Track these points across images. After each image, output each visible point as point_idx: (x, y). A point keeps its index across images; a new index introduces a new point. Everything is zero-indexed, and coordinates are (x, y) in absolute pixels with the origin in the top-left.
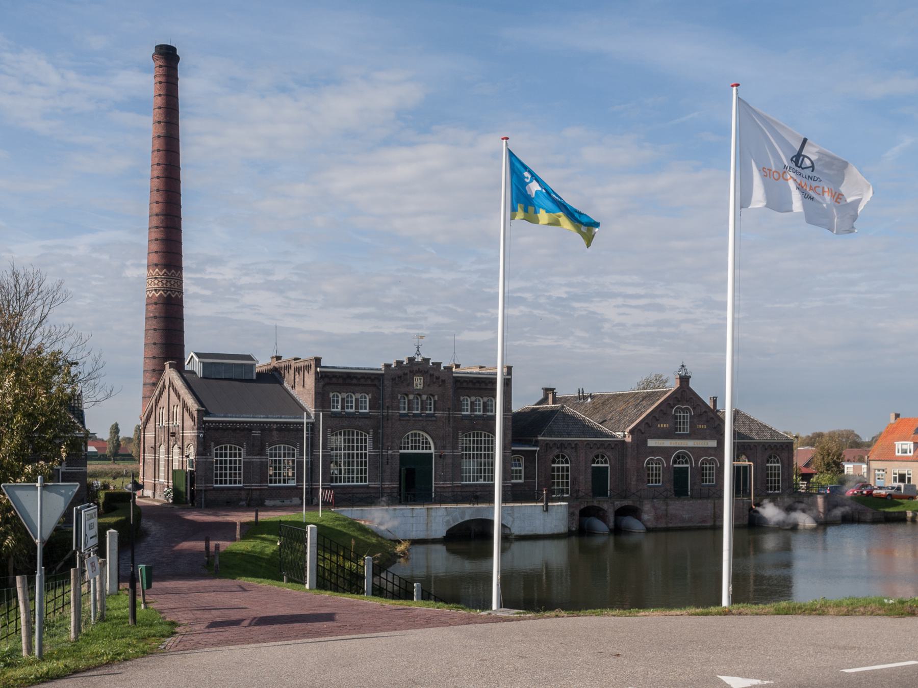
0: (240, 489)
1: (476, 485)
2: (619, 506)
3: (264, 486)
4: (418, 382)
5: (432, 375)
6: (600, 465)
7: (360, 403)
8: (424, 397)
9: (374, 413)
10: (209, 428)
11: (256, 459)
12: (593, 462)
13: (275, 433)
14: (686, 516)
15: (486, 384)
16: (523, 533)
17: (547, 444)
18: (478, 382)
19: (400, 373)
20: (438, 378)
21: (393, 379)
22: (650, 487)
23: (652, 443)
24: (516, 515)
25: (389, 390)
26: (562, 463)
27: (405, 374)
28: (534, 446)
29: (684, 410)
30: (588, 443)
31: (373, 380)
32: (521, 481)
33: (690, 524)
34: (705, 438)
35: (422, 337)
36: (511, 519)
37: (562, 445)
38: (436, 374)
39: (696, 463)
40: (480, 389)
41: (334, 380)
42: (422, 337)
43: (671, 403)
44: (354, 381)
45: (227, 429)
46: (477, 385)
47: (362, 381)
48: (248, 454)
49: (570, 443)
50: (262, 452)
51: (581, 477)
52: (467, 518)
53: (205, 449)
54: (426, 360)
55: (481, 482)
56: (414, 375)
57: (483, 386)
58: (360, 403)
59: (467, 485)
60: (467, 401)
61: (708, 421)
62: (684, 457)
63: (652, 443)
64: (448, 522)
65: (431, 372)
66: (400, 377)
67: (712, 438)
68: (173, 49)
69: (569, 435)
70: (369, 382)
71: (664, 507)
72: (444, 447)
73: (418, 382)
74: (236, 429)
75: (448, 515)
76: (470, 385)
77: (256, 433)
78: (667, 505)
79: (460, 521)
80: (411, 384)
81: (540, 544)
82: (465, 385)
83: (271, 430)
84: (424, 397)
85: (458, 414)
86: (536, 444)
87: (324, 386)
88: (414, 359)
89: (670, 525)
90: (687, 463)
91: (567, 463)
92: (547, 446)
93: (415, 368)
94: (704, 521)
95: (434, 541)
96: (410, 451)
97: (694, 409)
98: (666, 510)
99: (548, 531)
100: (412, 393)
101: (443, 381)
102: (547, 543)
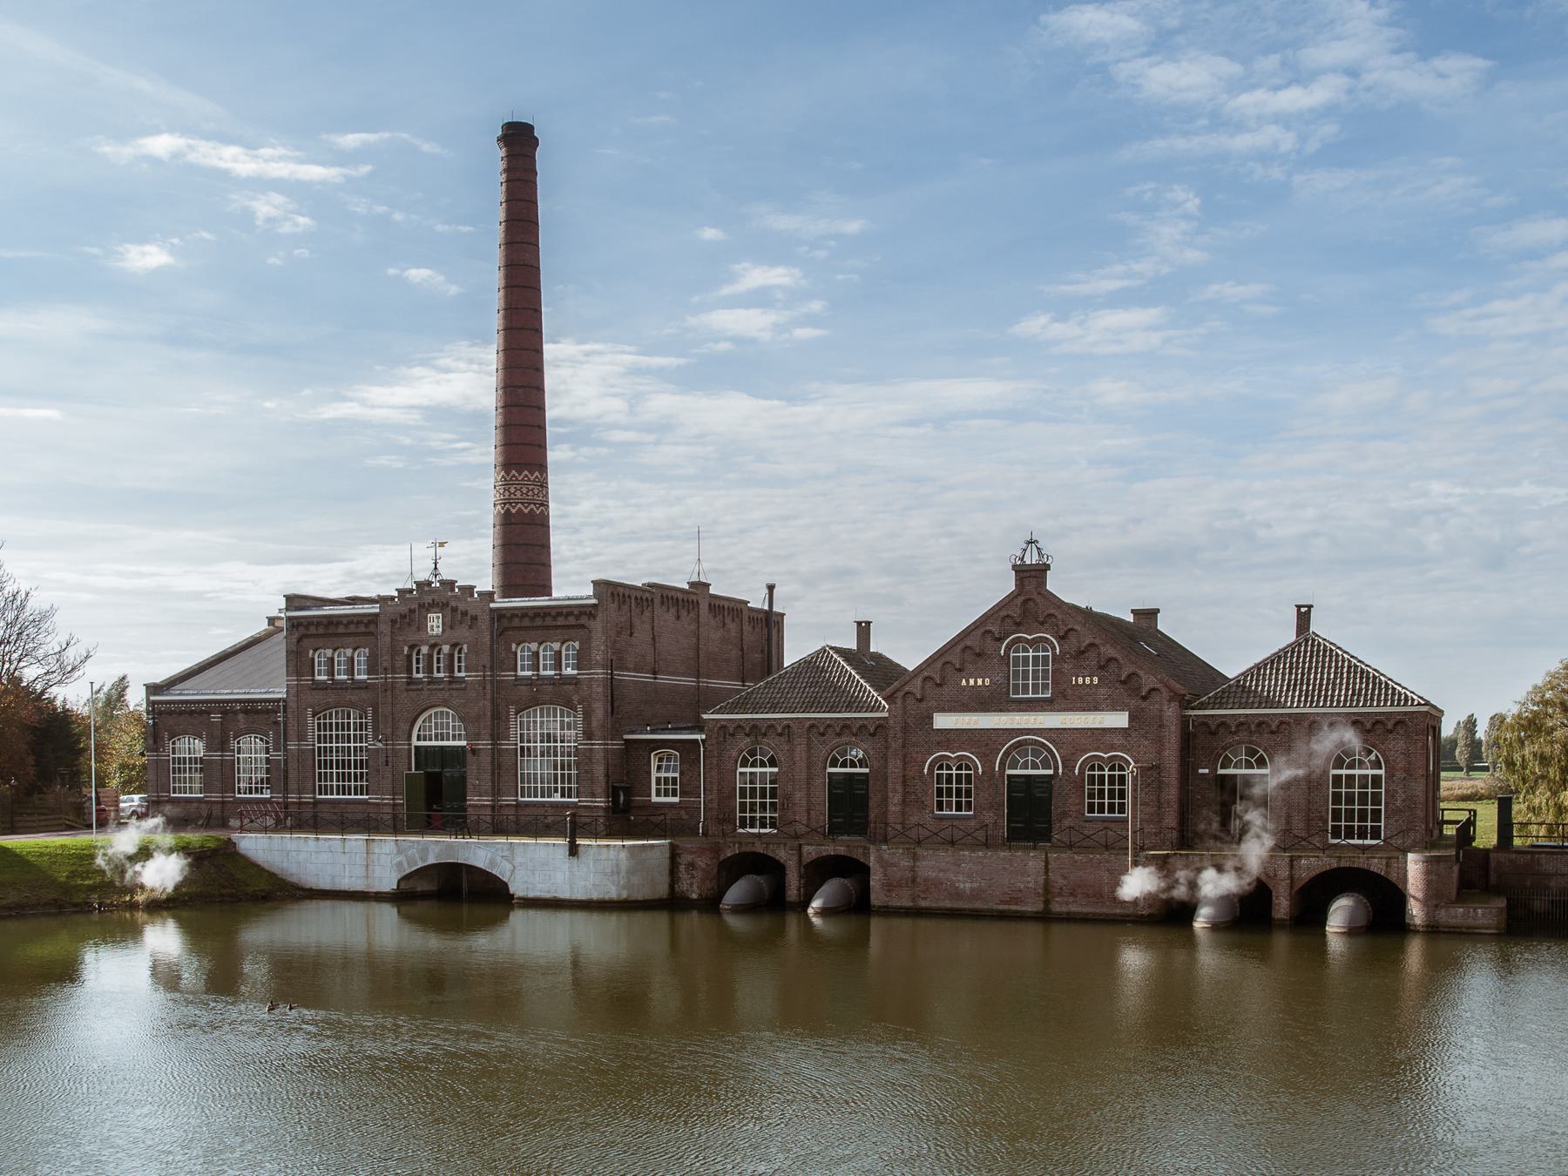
0: (198, 800)
1: (543, 804)
2: (814, 856)
3: (229, 797)
4: (435, 623)
5: (455, 610)
6: (848, 770)
7: (349, 664)
8: (446, 649)
9: (378, 679)
10: (161, 713)
11: (216, 756)
12: (834, 765)
13: (241, 716)
14: (966, 886)
15: (555, 618)
16: (531, 895)
17: (723, 727)
18: (537, 615)
19: (404, 609)
20: (465, 614)
21: (393, 622)
22: (942, 818)
23: (943, 721)
24: (518, 860)
25: (388, 639)
26: (763, 765)
27: (412, 611)
28: (691, 729)
29: (1033, 643)
30: (813, 726)
31: (367, 625)
32: (676, 800)
33: (978, 905)
34: (1096, 708)
35: (442, 545)
36: (508, 866)
37: (755, 729)
38: (462, 606)
39: (1068, 766)
40: (548, 628)
41: (313, 630)
42: (442, 545)
43: (995, 629)
44: (341, 630)
45: (181, 713)
46: (538, 622)
47: (352, 628)
48: (208, 748)
49: (771, 725)
50: (223, 746)
51: (798, 795)
52: (432, 860)
53: (155, 742)
54: (450, 584)
55: (557, 798)
56: (428, 611)
57: (549, 621)
58: (349, 664)
59: (528, 804)
60: (523, 652)
61: (1102, 668)
62: (1036, 754)
63: (943, 721)
64: (400, 864)
65: (453, 604)
66: (403, 617)
67: (1114, 707)
68: (529, 128)
69: (773, 709)
70: (362, 629)
71: (905, 863)
72: (478, 736)
73: (435, 623)
74: (191, 713)
75: (399, 852)
76: (526, 622)
77: (216, 718)
78: (915, 858)
79: (420, 865)
80: (422, 626)
81: (565, 917)
82: (516, 622)
83: (235, 713)
84: (446, 649)
85: (508, 676)
86: (698, 726)
87: (299, 640)
88: (429, 583)
89: (923, 904)
90: (1046, 766)
91: (772, 763)
92: (725, 732)
93: (428, 599)
94: (1017, 901)
95: (379, 897)
96: (451, 743)
97: (1061, 639)
98: (913, 869)
99: (580, 895)
100: (423, 642)
101: (474, 618)
102: (580, 917)
